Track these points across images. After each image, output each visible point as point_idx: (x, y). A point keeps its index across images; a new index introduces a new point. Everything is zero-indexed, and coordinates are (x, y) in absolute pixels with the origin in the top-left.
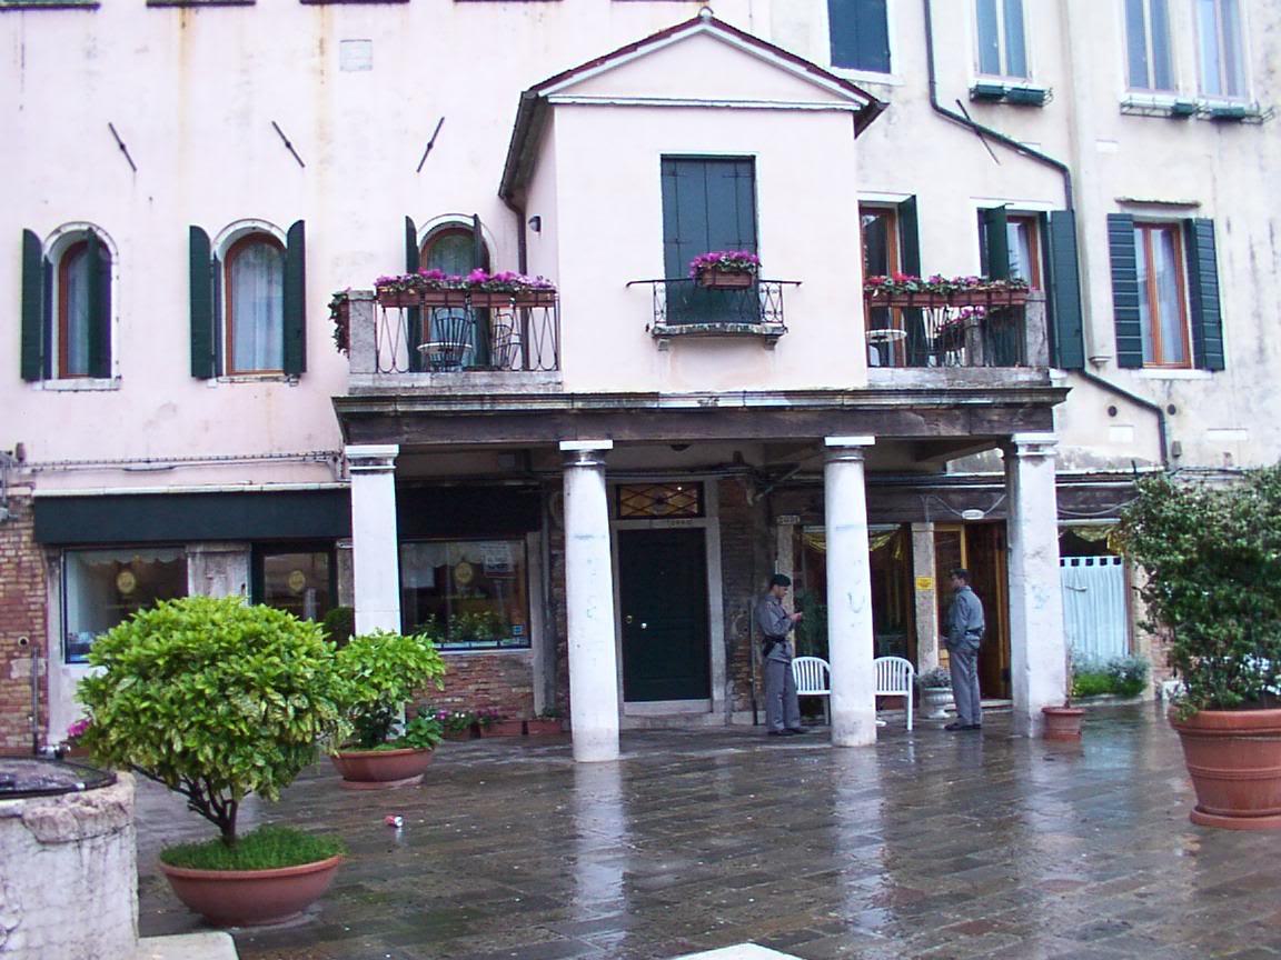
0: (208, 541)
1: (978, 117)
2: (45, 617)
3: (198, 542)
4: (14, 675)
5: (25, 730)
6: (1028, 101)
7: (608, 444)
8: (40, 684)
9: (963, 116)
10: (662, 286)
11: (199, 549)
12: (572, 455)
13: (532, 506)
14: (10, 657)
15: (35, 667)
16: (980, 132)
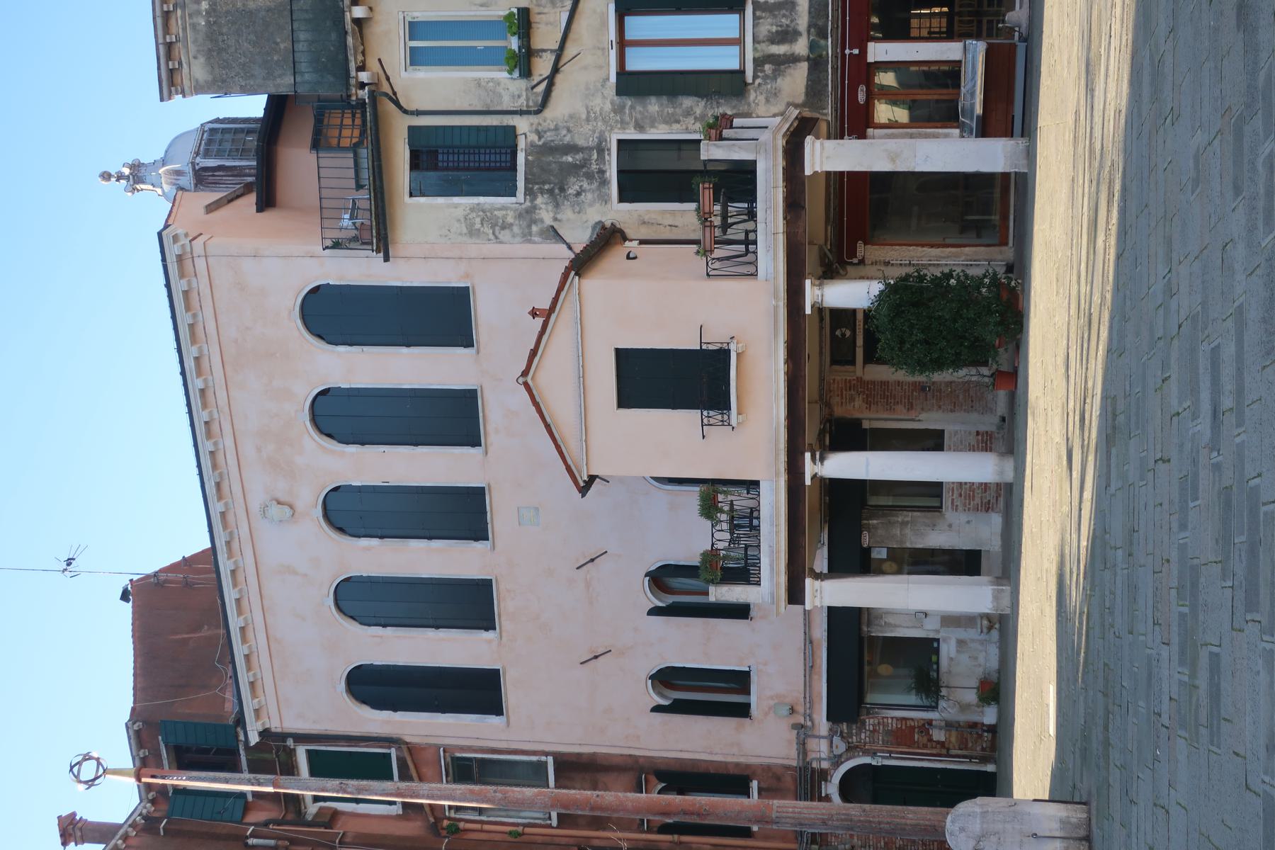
0: (860, 624)
1: (542, 66)
2: (905, 719)
3: (860, 629)
4: (943, 739)
5: (980, 736)
6: (523, 22)
7: (808, 455)
8: (949, 725)
9: (545, 83)
10: (705, 413)
11: (865, 629)
12: (814, 477)
13: (847, 501)
14: (930, 740)
15: (941, 728)
16: (556, 70)
